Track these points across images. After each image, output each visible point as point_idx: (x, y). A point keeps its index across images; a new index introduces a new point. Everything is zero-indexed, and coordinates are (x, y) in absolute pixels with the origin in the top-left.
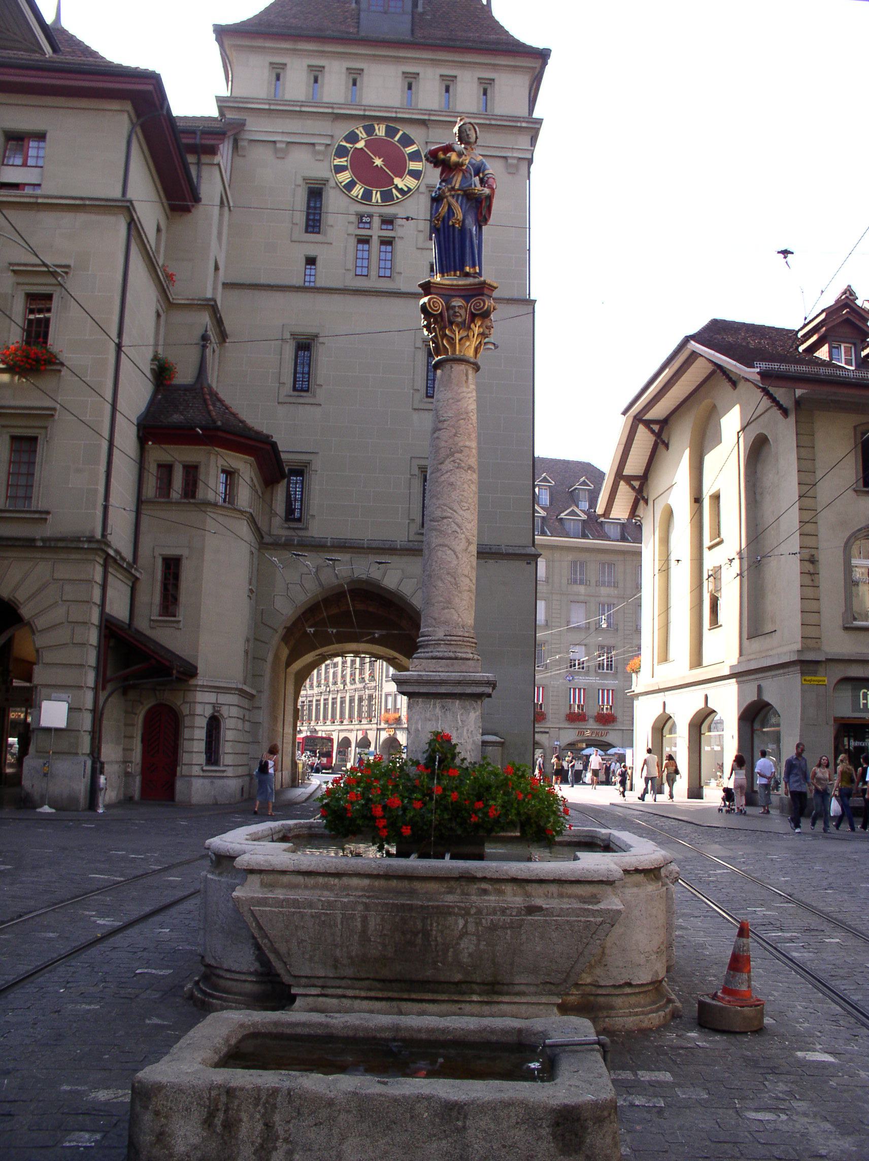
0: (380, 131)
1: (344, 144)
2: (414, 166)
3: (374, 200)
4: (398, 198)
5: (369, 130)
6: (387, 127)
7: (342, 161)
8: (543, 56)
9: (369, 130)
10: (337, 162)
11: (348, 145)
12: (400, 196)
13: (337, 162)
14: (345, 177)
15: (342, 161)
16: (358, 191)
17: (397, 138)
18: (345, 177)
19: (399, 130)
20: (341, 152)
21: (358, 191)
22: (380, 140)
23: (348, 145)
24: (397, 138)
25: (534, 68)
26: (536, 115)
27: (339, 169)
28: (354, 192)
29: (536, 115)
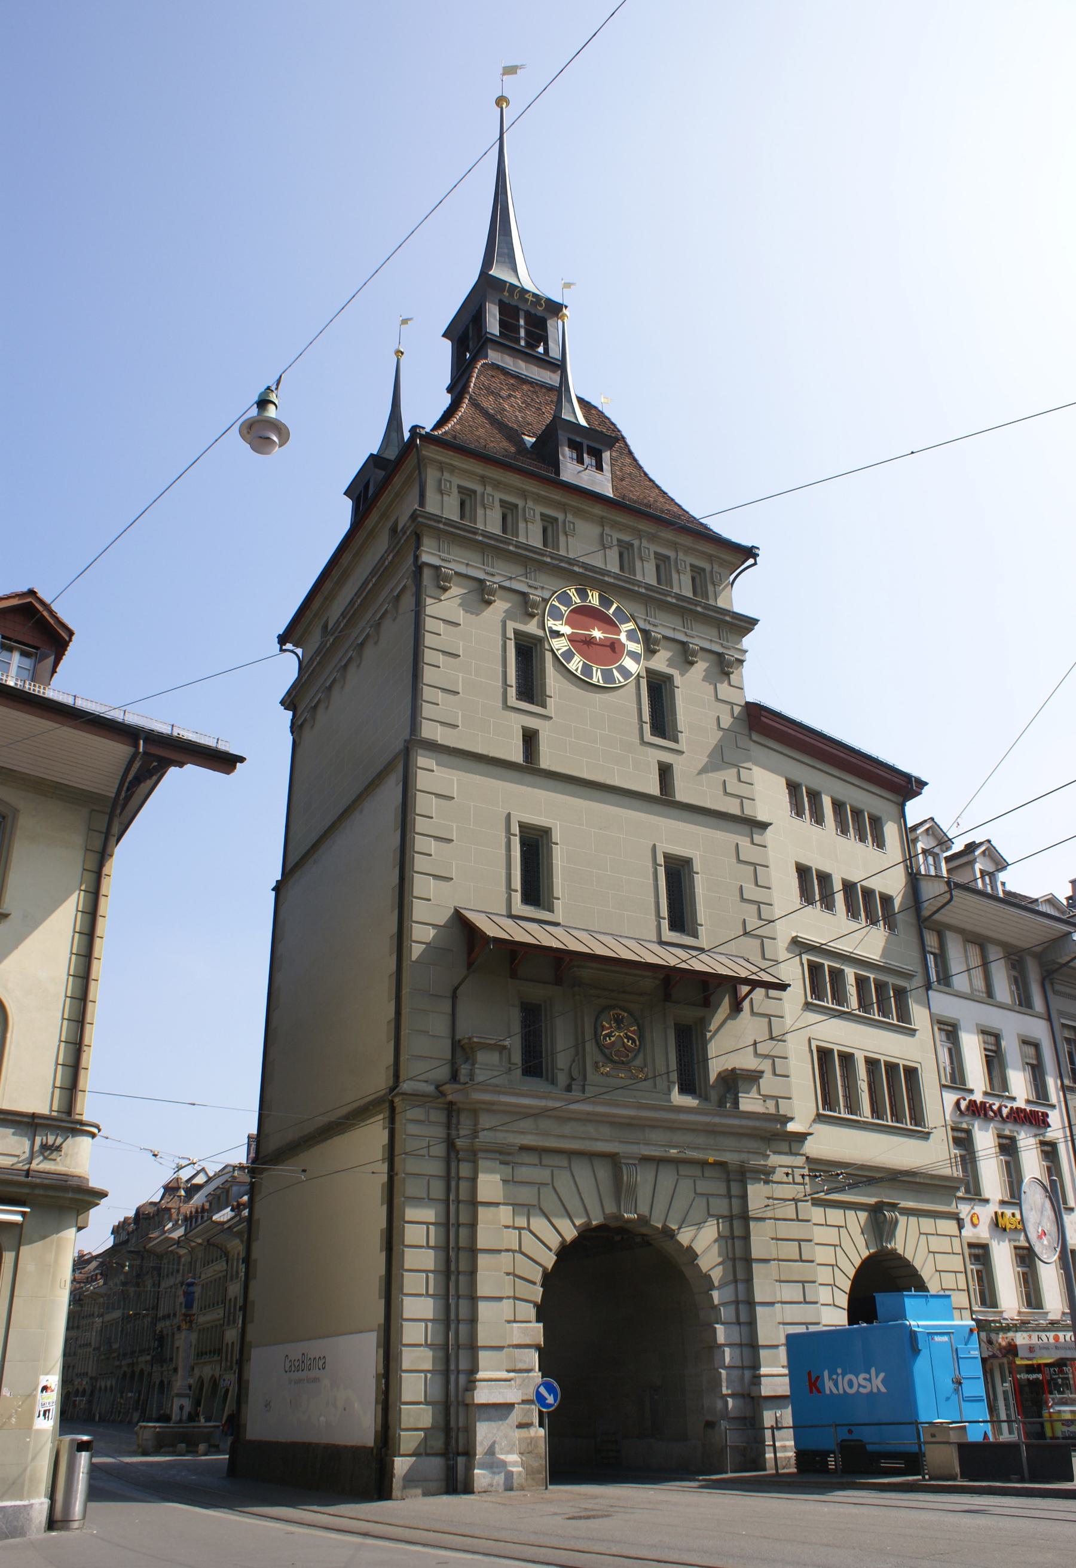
1: (557, 604)
5: (583, 594)
11: (561, 607)
12: (622, 680)
17: (611, 611)
19: (612, 603)
24: (611, 611)
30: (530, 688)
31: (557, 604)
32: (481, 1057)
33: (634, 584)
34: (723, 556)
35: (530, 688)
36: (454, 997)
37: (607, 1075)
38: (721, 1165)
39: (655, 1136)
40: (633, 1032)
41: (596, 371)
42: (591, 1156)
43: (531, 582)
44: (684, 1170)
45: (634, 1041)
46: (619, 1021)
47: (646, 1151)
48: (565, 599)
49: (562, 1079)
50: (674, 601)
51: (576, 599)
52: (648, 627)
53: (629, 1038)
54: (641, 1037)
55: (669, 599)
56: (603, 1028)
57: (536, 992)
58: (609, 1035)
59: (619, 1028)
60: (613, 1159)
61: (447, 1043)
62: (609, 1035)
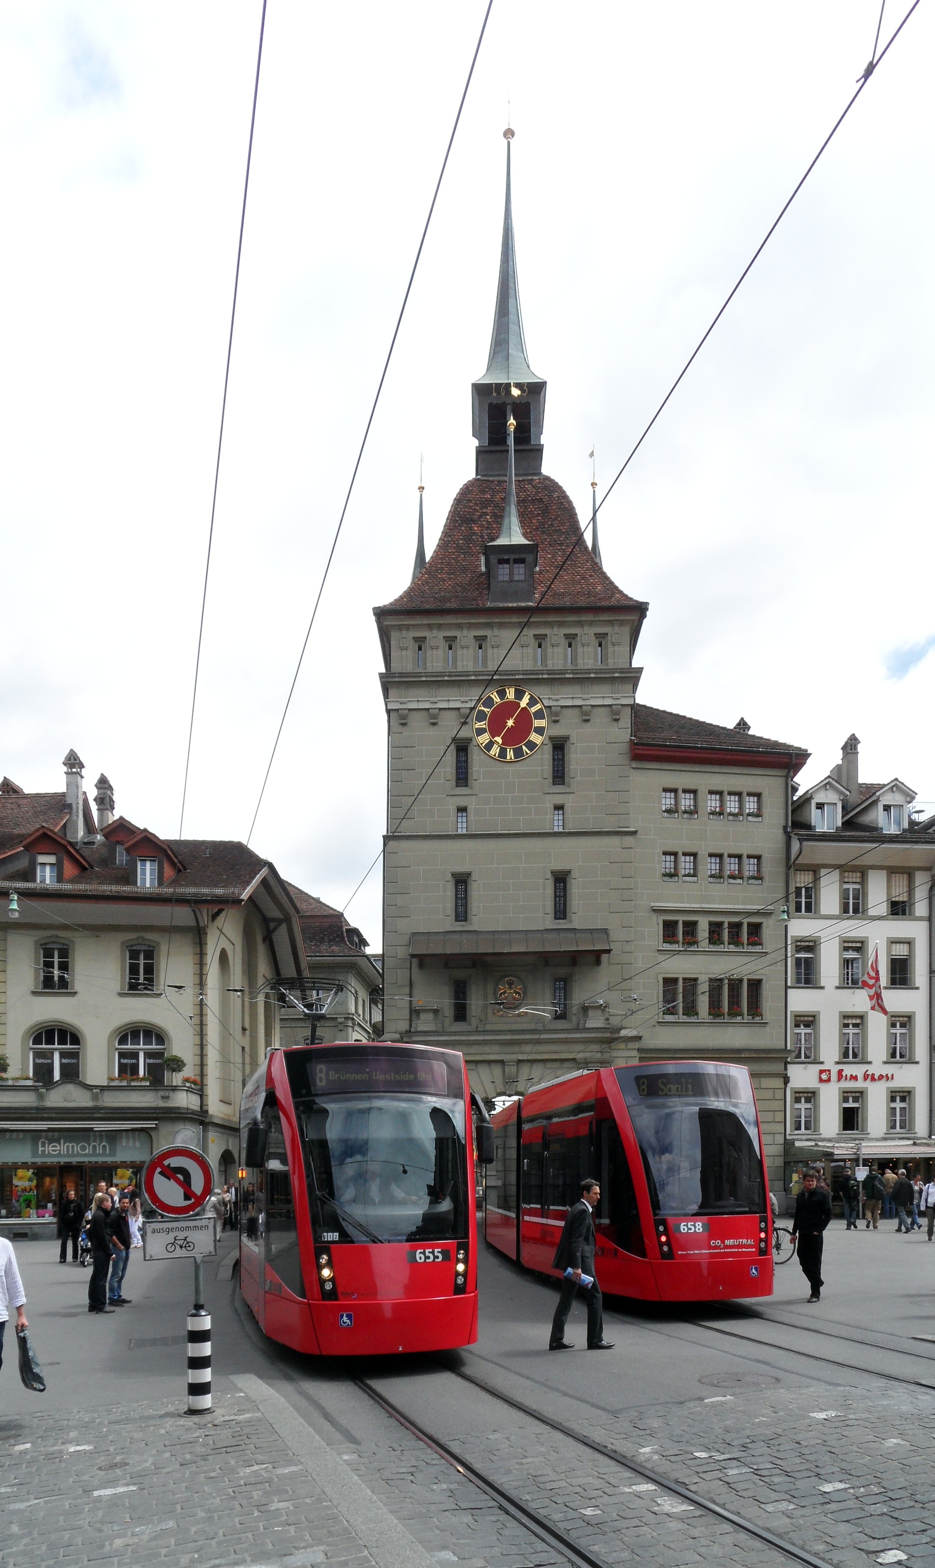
0: (511, 694)
1: (483, 708)
2: (537, 723)
3: (508, 758)
4: (527, 754)
5: (502, 694)
6: (516, 690)
7: (482, 725)
8: (640, 610)
9: (502, 694)
10: (478, 725)
11: (486, 710)
13: (478, 725)
14: (484, 739)
15: (482, 725)
16: (495, 751)
18: (484, 739)
20: (481, 716)
21: (495, 751)
22: (510, 703)
23: (486, 710)
25: (633, 621)
26: (635, 664)
27: (480, 732)
28: (492, 752)
29: (635, 664)
30: (462, 777)
31: (483, 708)
32: (423, 1016)
33: (538, 674)
34: (621, 618)
35: (462, 777)
36: (411, 985)
37: (502, 1016)
38: (574, 1060)
39: (527, 1048)
40: (520, 989)
41: (564, 456)
42: (490, 1062)
43: (462, 699)
44: (548, 1065)
45: (520, 994)
46: (510, 984)
47: (521, 1057)
48: (489, 702)
49: (474, 1022)
50: (571, 676)
51: (497, 699)
52: (551, 703)
53: (516, 993)
54: (525, 993)
55: (567, 676)
56: (500, 989)
57: (460, 974)
58: (504, 993)
59: (510, 988)
60: (502, 1062)
61: (408, 1012)
62: (504, 993)
